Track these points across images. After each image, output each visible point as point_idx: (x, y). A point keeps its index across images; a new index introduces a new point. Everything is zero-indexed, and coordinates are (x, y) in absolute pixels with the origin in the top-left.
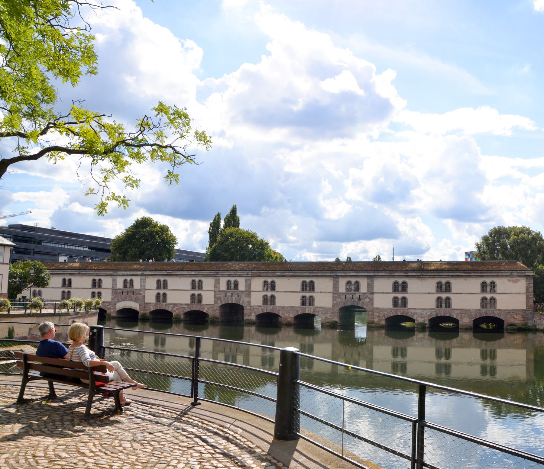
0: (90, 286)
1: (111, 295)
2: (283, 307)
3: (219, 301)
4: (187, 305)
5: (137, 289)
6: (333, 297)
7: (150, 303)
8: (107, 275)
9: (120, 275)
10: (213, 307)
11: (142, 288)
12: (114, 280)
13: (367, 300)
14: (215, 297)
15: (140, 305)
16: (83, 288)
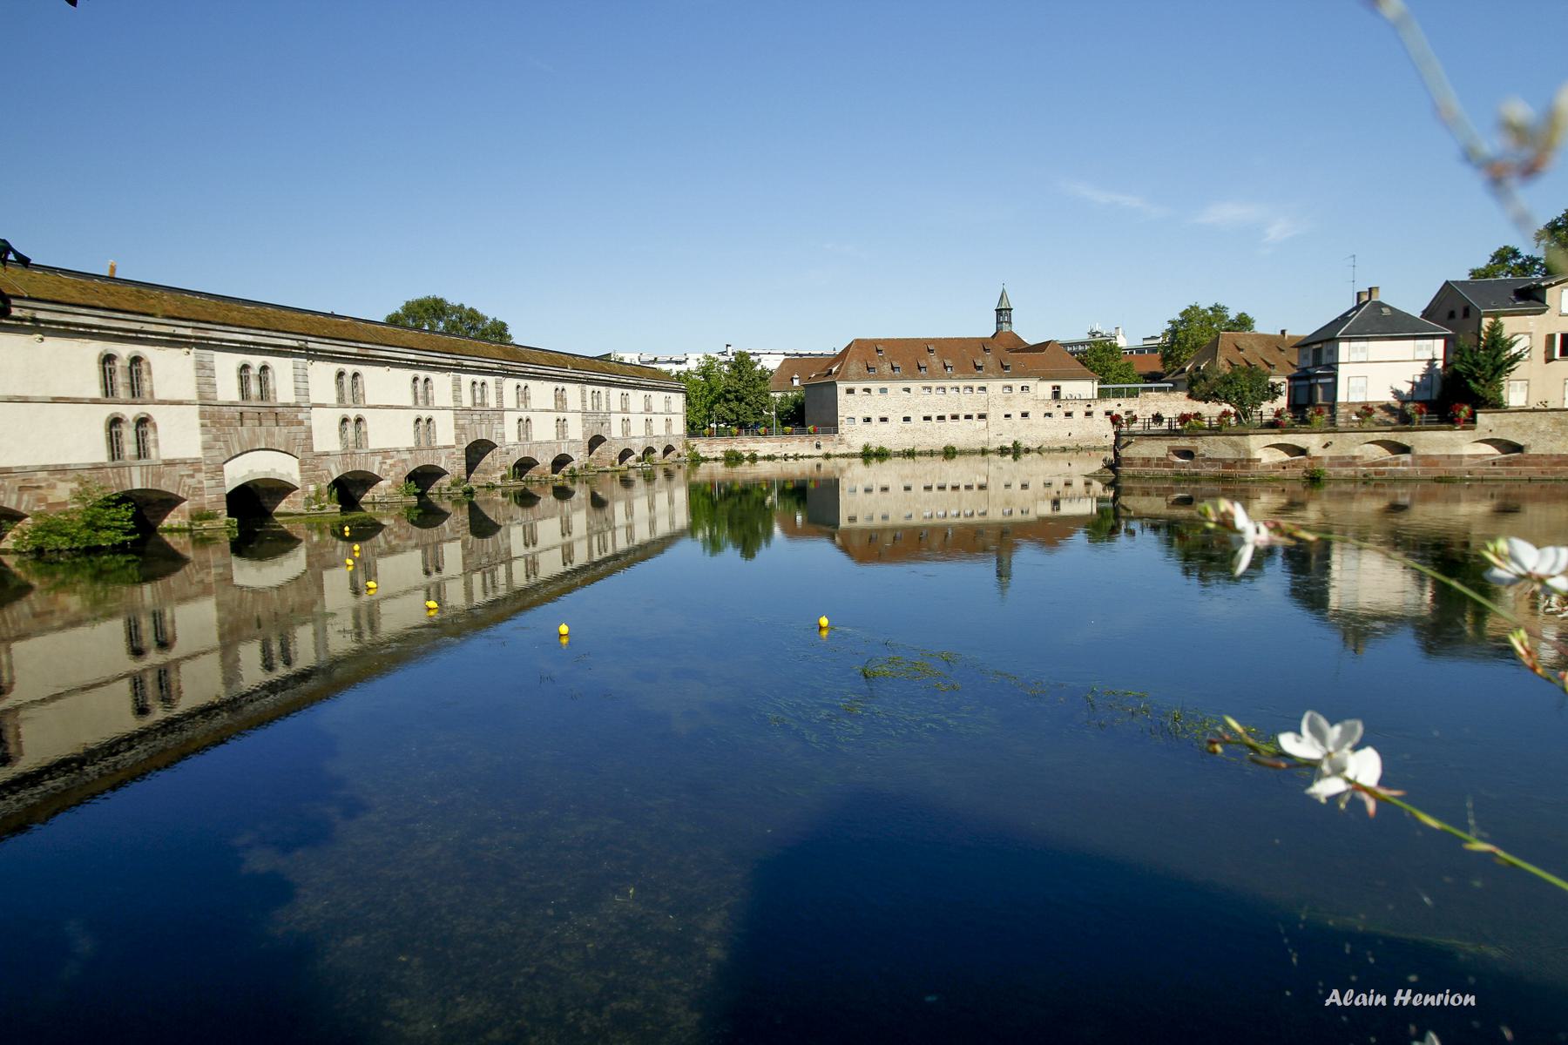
0: (96, 391)
1: (198, 430)
2: (541, 443)
3: (463, 436)
4: (410, 450)
5: (287, 406)
6: (583, 420)
7: (327, 454)
8: (174, 342)
9: (223, 346)
10: (453, 453)
11: (302, 399)
12: (201, 366)
13: (607, 425)
14: (457, 426)
15: (302, 464)
16: (55, 400)
